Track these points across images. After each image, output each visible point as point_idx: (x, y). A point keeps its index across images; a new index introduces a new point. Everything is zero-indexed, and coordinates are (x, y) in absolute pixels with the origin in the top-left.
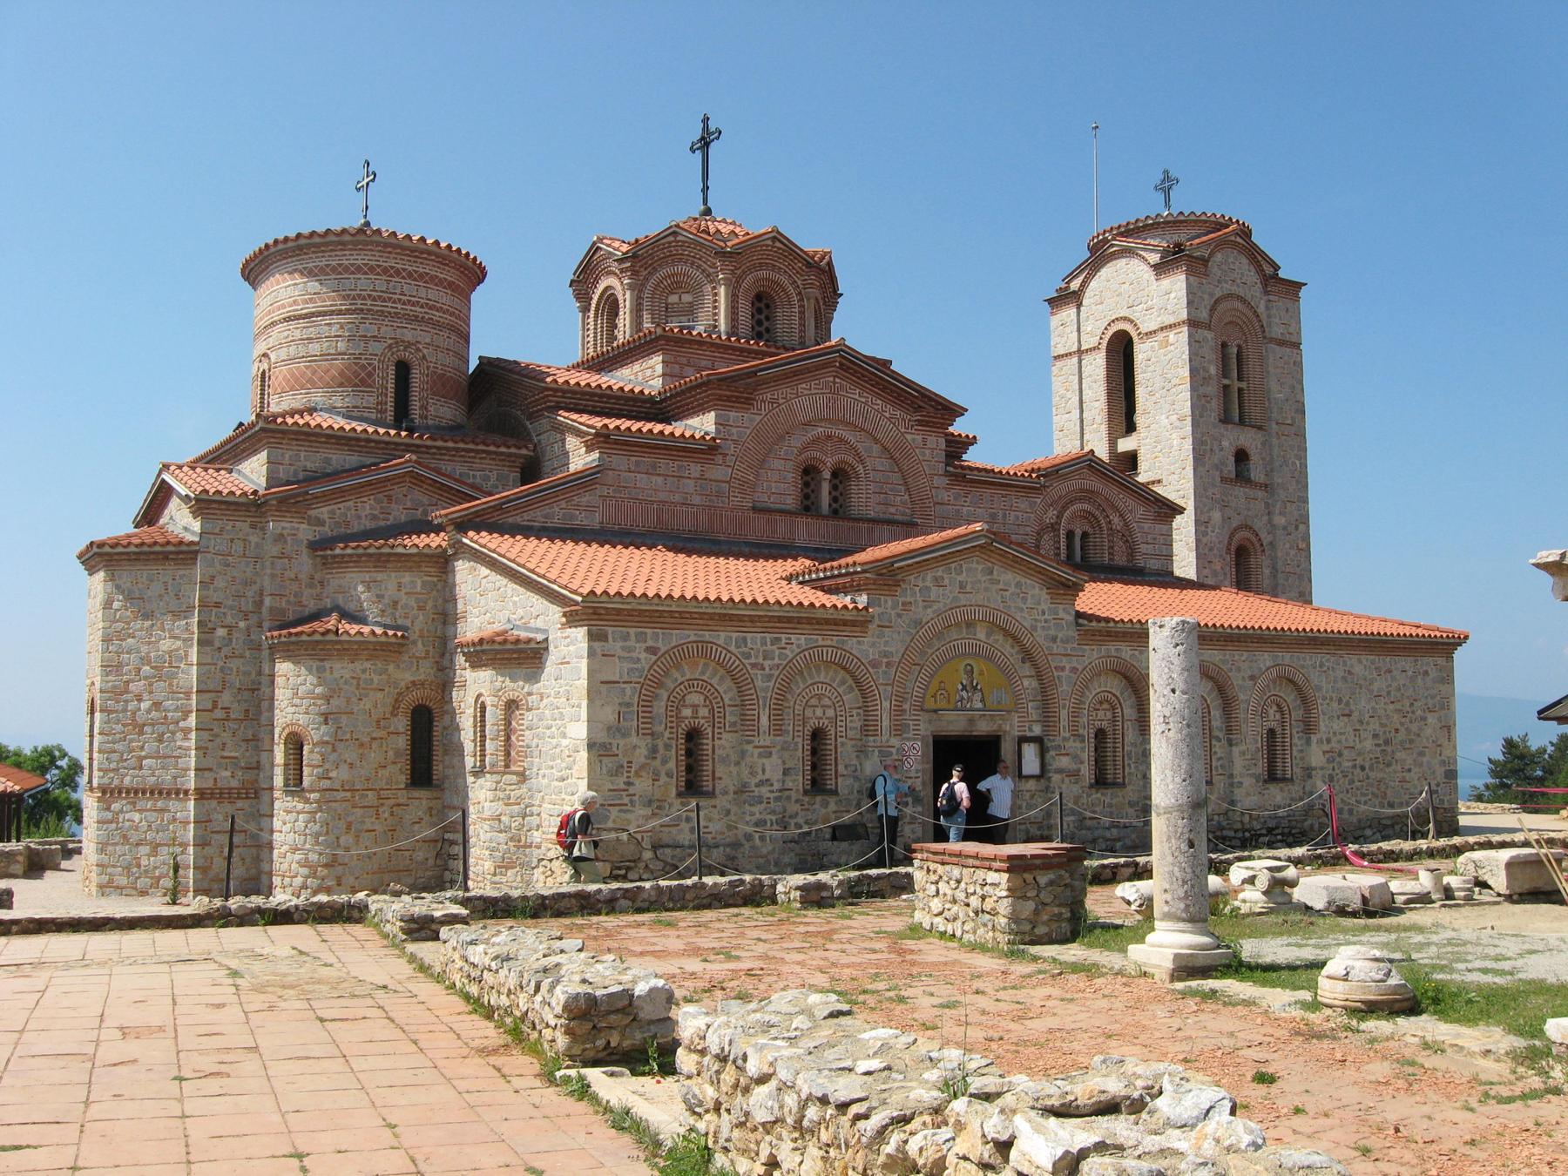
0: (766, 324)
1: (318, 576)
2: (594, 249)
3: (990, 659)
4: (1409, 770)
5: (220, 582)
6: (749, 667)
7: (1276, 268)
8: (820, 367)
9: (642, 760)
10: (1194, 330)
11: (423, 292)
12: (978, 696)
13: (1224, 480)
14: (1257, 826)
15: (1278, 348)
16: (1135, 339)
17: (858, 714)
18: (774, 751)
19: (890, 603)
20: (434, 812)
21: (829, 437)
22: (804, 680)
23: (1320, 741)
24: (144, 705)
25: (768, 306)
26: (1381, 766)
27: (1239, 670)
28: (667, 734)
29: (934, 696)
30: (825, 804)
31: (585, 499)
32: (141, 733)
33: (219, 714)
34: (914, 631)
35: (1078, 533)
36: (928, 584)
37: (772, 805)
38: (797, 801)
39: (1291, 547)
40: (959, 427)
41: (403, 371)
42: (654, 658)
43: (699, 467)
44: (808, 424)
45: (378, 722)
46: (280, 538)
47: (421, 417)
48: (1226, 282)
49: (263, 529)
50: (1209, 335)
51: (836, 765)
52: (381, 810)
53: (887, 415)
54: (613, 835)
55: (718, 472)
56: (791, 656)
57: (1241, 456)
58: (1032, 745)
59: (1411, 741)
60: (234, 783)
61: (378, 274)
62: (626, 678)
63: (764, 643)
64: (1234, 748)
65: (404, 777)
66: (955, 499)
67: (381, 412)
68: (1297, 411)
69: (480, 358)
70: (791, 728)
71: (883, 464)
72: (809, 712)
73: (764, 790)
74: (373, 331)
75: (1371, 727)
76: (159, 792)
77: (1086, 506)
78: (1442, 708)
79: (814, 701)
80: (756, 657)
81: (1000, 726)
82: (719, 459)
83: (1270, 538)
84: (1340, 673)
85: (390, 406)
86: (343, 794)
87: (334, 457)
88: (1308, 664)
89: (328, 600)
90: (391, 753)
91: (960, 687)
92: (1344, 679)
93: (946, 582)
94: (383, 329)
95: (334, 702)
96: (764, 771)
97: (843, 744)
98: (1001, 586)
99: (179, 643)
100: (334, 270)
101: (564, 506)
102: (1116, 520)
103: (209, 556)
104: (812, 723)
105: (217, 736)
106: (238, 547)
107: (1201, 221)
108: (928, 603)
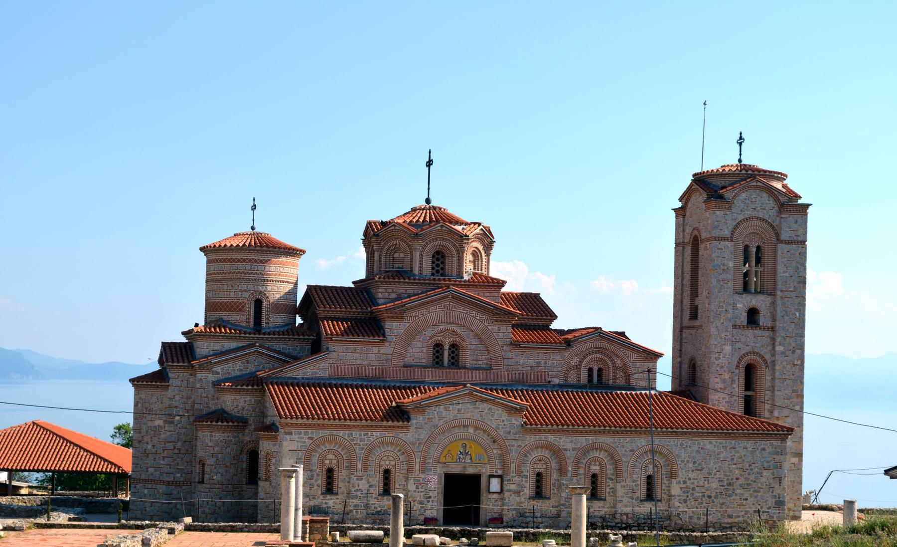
0: (441, 266)
1: (216, 396)
4: (747, 499)
5: (177, 398)
8: (443, 298)
12: (468, 457)
13: (735, 327)
14: (630, 521)
17: (406, 464)
22: (381, 450)
24: (149, 447)
25: (443, 257)
26: (724, 496)
28: (318, 470)
29: (445, 457)
32: (148, 456)
33: (176, 451)
36: (441, 410)
38: (375, 498)
42: (312, 441)
45: (234, 457)
47: (267, 323)
49: (195, 376)
53: (478, 318)
56: (373, 440)
59: (748, 485)
60: (182, 479)
61: (247, 262)
62: (299, 449)
63: (360, 435)
64: (618, 484)
65: (244, 480)
66: (516, 356)
68: (799, 282)
69: (308, 286)
71: (475, 341)
72: (382, 463)
73: (359, 493)
75: (718, 476)
76: (153, 481)
77: (599, 356)
80: (357, 441)
81: (480, 470)
82: (387, 344)
83: (773, 359)
84: (696, 448)
85: (252, 320)
86: (218, 486)
90: (239, 470)
91: (459, 453)
92: (698, 452)
93: (451, 409)
95: (216, 449)
96: (358, 486)
97: (398, 476)
98: (480, 410)
99: (162, 421)
100: (229, 260)
101: (312, 368)
102: (618, 362)
105: (175, 460)
106: (185, 383)
107: (736, 174)
108: (440, 418)
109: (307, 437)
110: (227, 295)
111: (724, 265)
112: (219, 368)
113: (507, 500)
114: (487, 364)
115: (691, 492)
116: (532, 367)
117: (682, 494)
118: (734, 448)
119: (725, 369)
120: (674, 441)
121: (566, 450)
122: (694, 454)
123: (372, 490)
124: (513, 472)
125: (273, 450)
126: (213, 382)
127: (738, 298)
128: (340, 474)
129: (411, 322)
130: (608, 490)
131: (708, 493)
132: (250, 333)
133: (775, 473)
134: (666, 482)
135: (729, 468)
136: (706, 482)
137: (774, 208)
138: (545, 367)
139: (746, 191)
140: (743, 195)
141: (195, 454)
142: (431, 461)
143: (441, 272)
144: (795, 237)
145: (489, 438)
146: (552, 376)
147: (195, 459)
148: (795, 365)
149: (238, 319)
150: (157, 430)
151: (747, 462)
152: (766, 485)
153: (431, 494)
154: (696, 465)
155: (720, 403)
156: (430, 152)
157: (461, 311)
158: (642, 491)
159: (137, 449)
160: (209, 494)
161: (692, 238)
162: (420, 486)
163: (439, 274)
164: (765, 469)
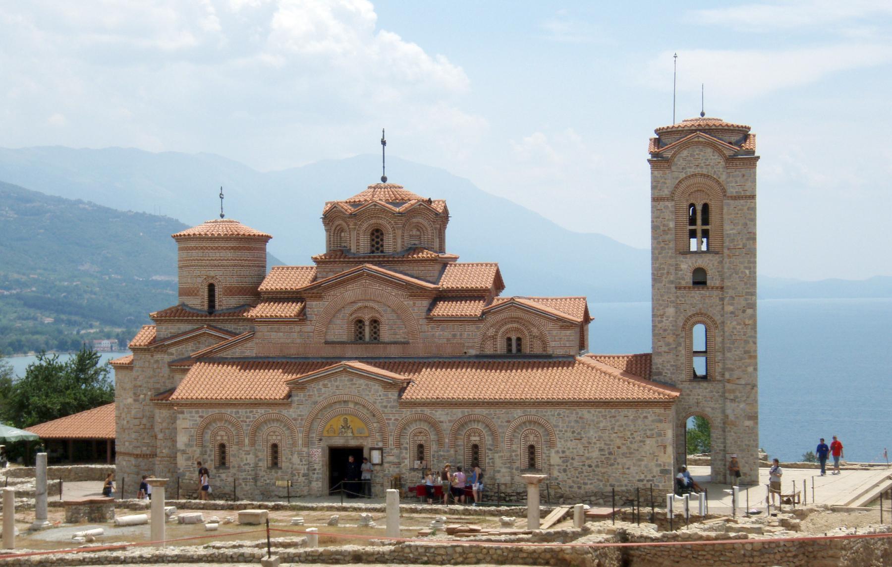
1: (171, 375)
3: (356, 416)
4: (628, 468)
5: (141, 378)
8: (359, 276)
9: (198, 455)
10: (656, 204)
11: (218, 255)
12: (350, 431)
15: (732, 202)
18: (251, 452)
19: (302, 396)
21: (366, 307)
23: (558, 452)
24: (125, 422)
25: (382, 234)
26: (605, 465)
27: (499, 418)
28: (211, 446)
30: (277, 473)
31: (249, 344)
32: (124, 431)
33: (142, 426)
34: (314, 406)
35: (514, 338)
37: (250, 472)
39: (739, 324)
41: (211, 288)
42: (202, 419)
43: (299, 327)
44: (354, 302)
46: (157, 361)
48: (690, 168)
50: (670, 204)
53: (394, 294)
54: (188, 481)
55: (308, 328)
59: (631, 453)
60: (148, 452)
67: (203, 305)
68: (748, 239)
72: (269, 438)
73: (247, 467)
75: (598, 445)
77: (515, 325)
78: (660, 435)
79: (272, 434)
84: (573, 417)
86: (167, 458)
88: (550, 415)
92: (577, 421)
93: (329, 385)
94: (202, 272)
96: (247, 460)
98: (357, 386)
102: (535, 331)
104: (272, 442)
106: (147, 364)
107: (679, 131)
109: (198, 415)
111: (664, 225)
112: (174, 349)
113: (387, 471)
114: (405, 338)
115: (571, 461)
116: (448, 340)
117: (562, 464)
118: (614, 417)
119: (669, 331)
120: (551, 411)
121: (442, 422)
122: (572, 424)
123: (260, 464)
124: (391, 444)
126: (169, 362)
127: (682, 259)
128: (231, 449)
129: (329, 300)
130: (487, 461)
131: (588, 462)
132: (206, 316)
133: (659, 441)
134: (546, 451)
135: (610, 437)
136: (586, 452)
137: (720, 162)
138: (461, 339)
139: (688, 147)
140: (685, 153)
142: (314, 435)
143: (381, 249)
144: (743, 192)
146: (469, 347)
148: (746, 325)
151: (629, 430)
152: (650, 454)
153: (316, 466)
154: (575, 435)
155: (665, 367)
156: (383, 131)
157: (377, 288)
158: (524, 461)
160: (160, 466)
162: (303, 460)
163: (379, 251)
164: (648, 437)
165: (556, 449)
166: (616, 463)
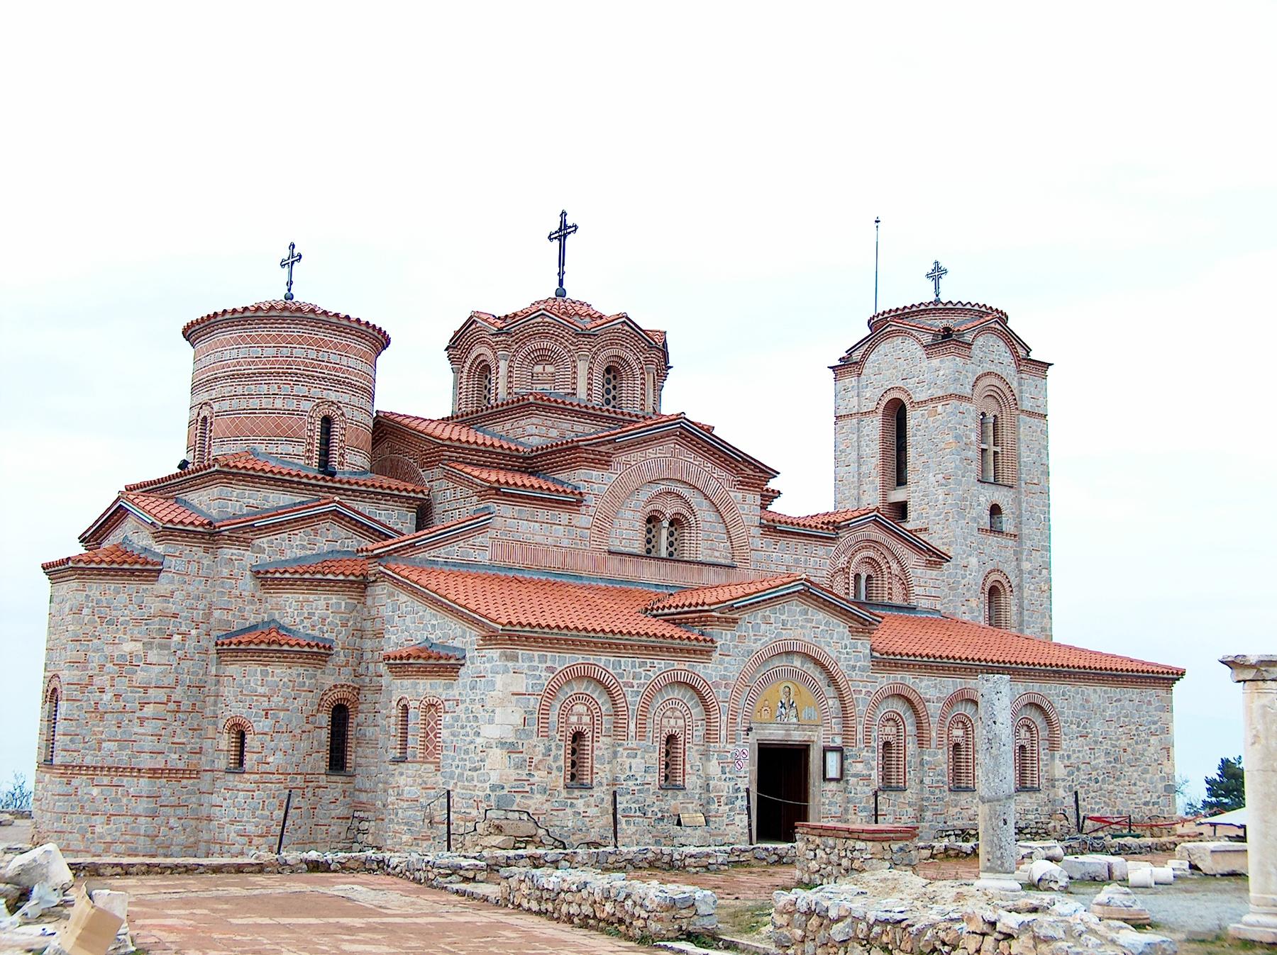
1: (258, 594)
2: (471, 321)
4: (1135, 784)
6: (622, 685)
7: (1028, 350)
9: (540, 757)
12: (793, 712)
16: (908, 407)
18: (639, 752)
19: (729, 636)
20: (347, 794)
23: (1062, 757)
24: (107, 697)
28: (558, 737)
31: (479, 540)
32: (102, 719)
33: (172, 706)
35: (864, 576)
40: (773, 484)
51: (684, 766)
52: (306, 790)
53: (715, 476)
55: (582, 520)
56: (654, 677)
57: (995, 510)
58: (835, 753)
60: (181, 765)
63: (633, 666)
65: (323, 764)
66: (768, 546)
67: (308, 458)
70: (651, 734)
71: (712, 516)
73: (630, 783)
74: (304, 391)
78: (1162, 733)
85: (316, 455)
86: (276, 776)
87: (272, 495)
88: (1053, 692)
89: (266, 615)
90: (315, 743)
91: (780, 705)
93: (772, 620)
94: (313, 389)
95: (275, 699)
99: (140, 645)
101: (462, 545)
103: (170, 575)
104: (667, 731)
109: (544, 666)
110: (268, 403)
112: (265, 540)
116: (787, 566)
121: (928, 701)
125: (443, 698)
126: (253, 566)
134: (1043, 757)
140: (981, 339)
141: (214, 711)
145: (822, 677)
147: (215, 724)
149: (291, 452)
150: (126, 665)
154: (1080, 729)
159: (79, 703)
161: (883, 403)
162: (727, 770)
164: (1152, 734)
165: (1061, 753)
166: (1122, 775)
